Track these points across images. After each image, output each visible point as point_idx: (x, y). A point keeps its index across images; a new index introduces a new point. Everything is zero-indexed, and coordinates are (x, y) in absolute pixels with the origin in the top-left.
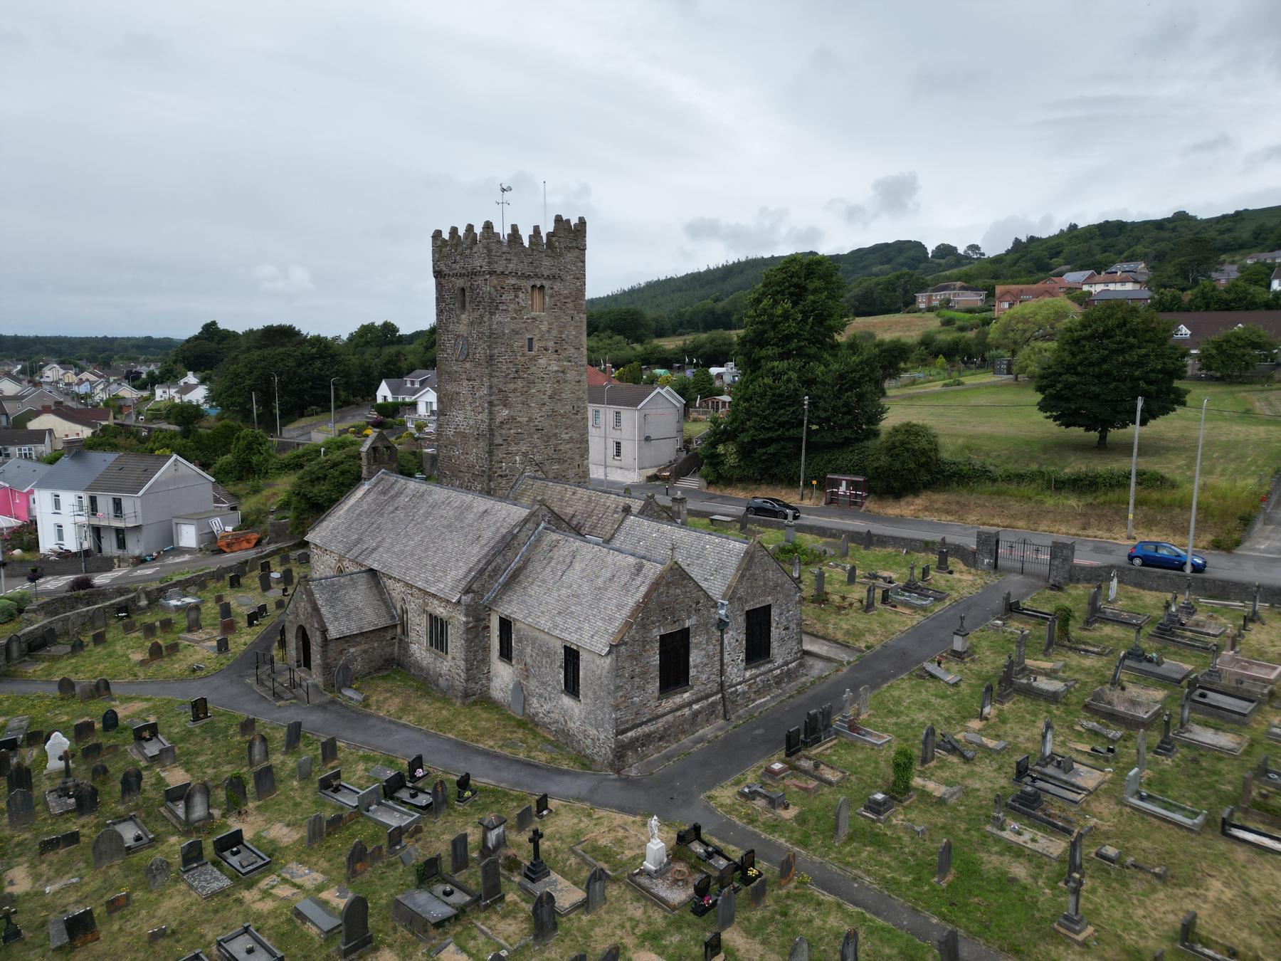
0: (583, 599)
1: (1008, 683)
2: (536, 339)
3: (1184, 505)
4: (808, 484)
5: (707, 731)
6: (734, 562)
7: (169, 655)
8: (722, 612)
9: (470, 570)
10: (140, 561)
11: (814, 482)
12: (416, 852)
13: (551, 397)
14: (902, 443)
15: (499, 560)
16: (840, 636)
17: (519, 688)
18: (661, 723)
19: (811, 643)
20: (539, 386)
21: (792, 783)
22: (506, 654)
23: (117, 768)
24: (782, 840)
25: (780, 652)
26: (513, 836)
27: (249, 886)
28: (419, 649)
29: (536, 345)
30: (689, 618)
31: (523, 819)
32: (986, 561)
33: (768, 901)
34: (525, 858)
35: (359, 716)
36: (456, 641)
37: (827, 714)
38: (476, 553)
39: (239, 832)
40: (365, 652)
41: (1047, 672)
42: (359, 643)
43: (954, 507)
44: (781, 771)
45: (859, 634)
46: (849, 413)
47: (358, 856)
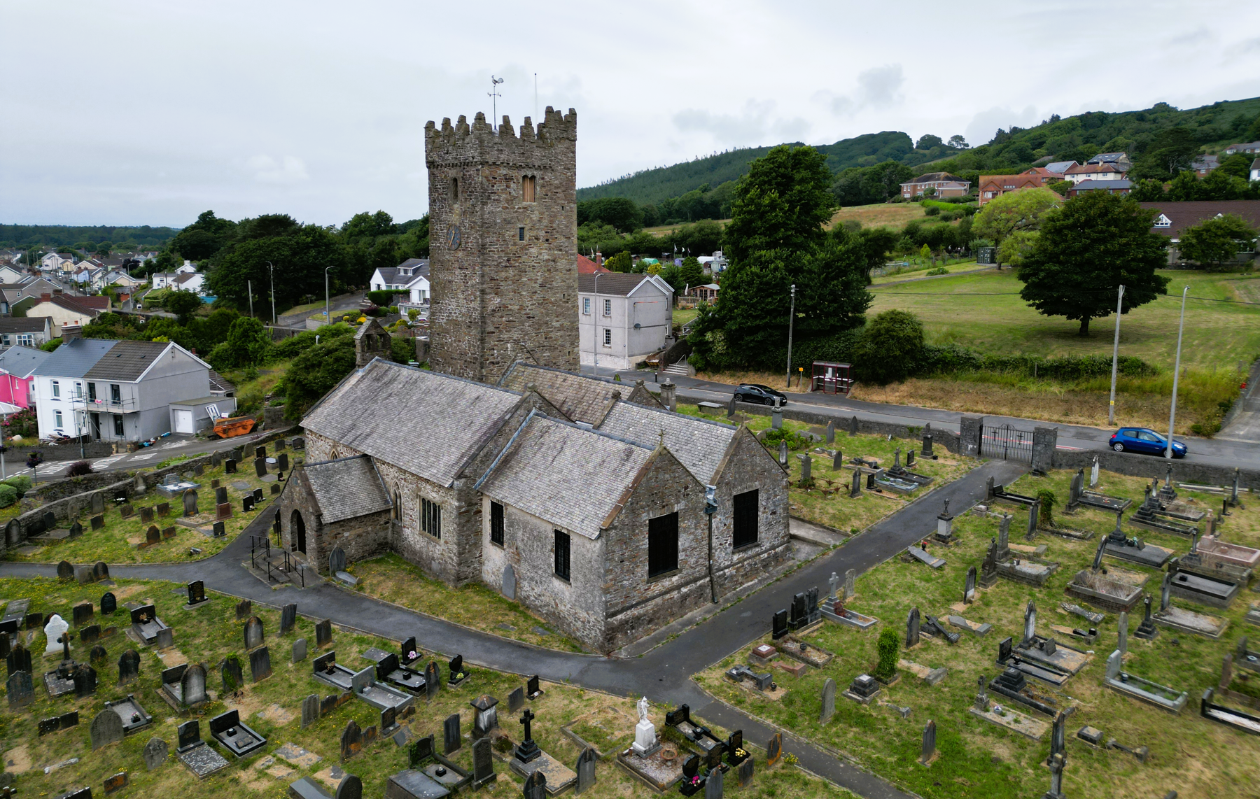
0: (573, 484)
1: (992, 567)
2: (527, 228)
3: (1165, 391)
4: (794, 372)
5: (696, 613)
6: (721, 448)
7: (166, 539)
8: (710, 497)
9: (463, 456)
10: (138, 447)
11: (801, 369)
12: (411, 732)
13: (542, 286)
14: (887, 331)
15: (491, 445)
16: (826, 521)
17: (510, 571)
18: (650, 606)
19: (798, 527)
20: (530, 275)
21: (779, 665)
22: (498, 538)
23: (115, 650)
24: (769, 721)
25: (767, 536)
26: (505, 717)
27: (245, 767)
28: (413, 533)
29: (527, 235)
30: (678, 503)
31: (515, 700)
32: (970, 446)
33: (756, 780)
34: (517, 738)
35: (353, 600)
36: (448, 525)
37: (813, 598)
38: (468, 439)
39: (235, 713)
40: (359, 536)
42: (352, 528)
43: (939, 394)
44: (768, 653)
45: (845, 519)
46: (835, 300)
47: (352, 737)
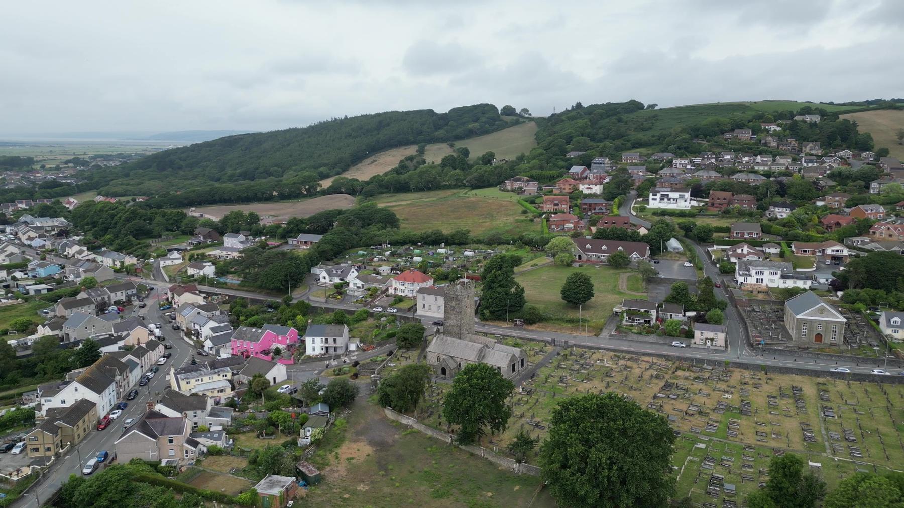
1: (559, 367)
25: (525, 365)
41: (564, 364)
